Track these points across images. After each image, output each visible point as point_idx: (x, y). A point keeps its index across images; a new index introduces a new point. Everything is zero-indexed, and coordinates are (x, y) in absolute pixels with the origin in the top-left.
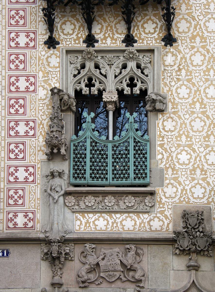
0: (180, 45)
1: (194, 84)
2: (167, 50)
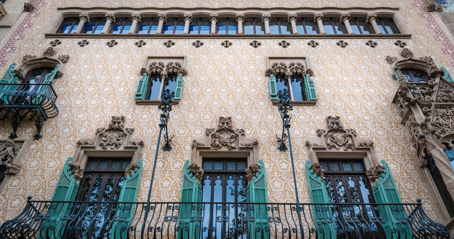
0: (43, 140)
1: (42, 160)
2: (34, 142)
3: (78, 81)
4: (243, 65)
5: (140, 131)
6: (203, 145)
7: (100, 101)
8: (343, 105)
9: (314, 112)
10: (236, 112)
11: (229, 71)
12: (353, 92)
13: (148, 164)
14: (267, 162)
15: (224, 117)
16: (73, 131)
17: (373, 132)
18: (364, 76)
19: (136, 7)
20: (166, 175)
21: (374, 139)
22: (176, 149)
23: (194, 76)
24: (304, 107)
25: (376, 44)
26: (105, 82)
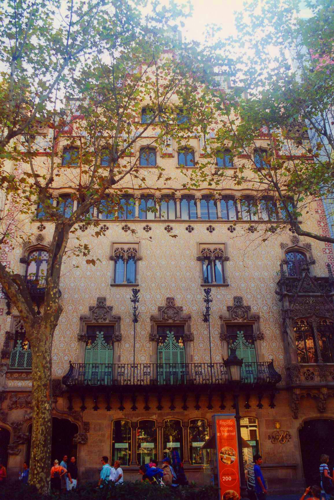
24: (221, 288)
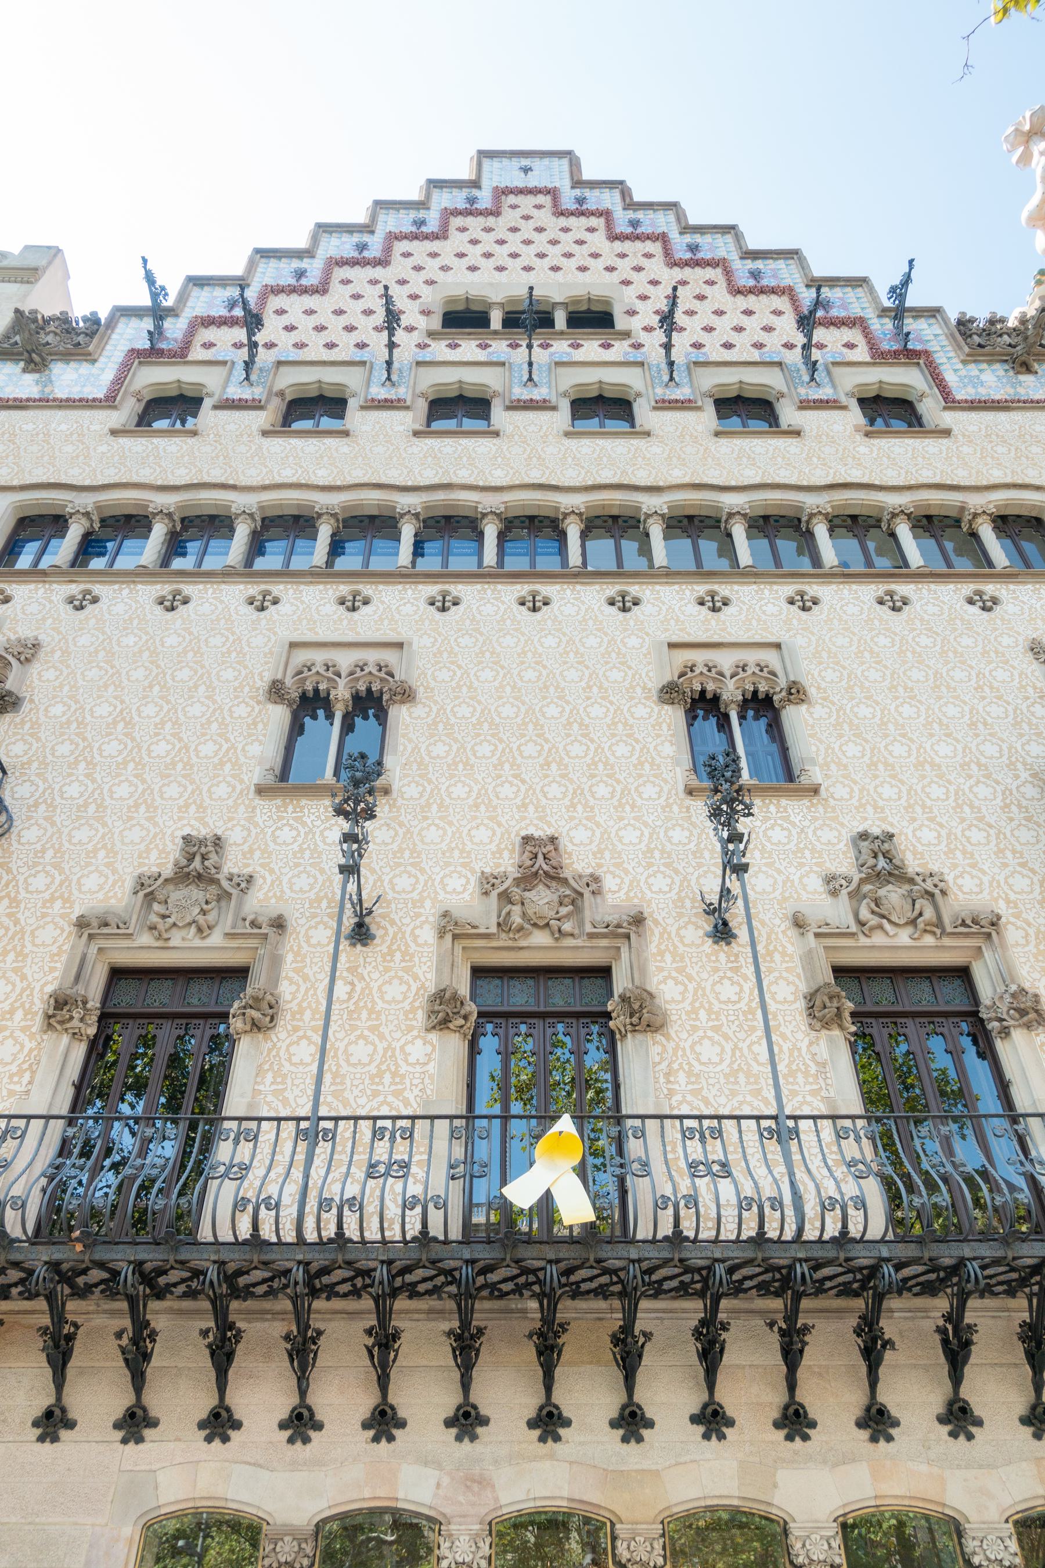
3: (69, 722)
4: (587, 668)
5: (273, 882)
6: (474, 927)
7: (141, 788)
8: (904, 794)
9: (816, 819)
10: (572, 818)
11: (546, 687)
12: (932, 754)
13: (303, 989)
14: (674, 979)
15: (536, 835)
16: (61, 885)
17: (998, 882)
18: (965, 703)
19: (243, 481)
20: (358, 1023)
21: (1002, 904)
22: (388, 939)
23: (436, 702)
24: (784, 802)
25: (995, 601)
26: (156, 725)
